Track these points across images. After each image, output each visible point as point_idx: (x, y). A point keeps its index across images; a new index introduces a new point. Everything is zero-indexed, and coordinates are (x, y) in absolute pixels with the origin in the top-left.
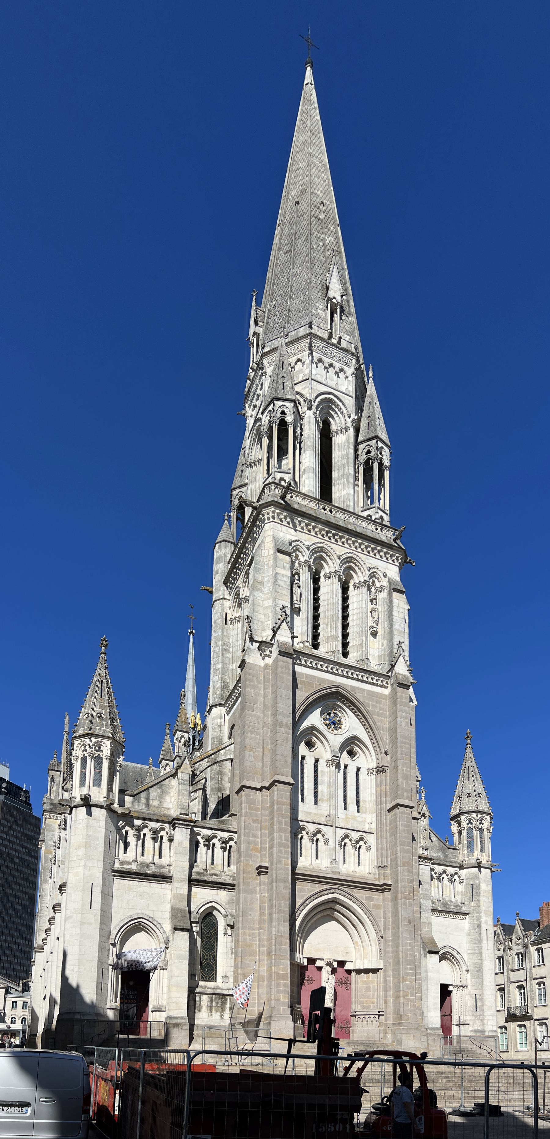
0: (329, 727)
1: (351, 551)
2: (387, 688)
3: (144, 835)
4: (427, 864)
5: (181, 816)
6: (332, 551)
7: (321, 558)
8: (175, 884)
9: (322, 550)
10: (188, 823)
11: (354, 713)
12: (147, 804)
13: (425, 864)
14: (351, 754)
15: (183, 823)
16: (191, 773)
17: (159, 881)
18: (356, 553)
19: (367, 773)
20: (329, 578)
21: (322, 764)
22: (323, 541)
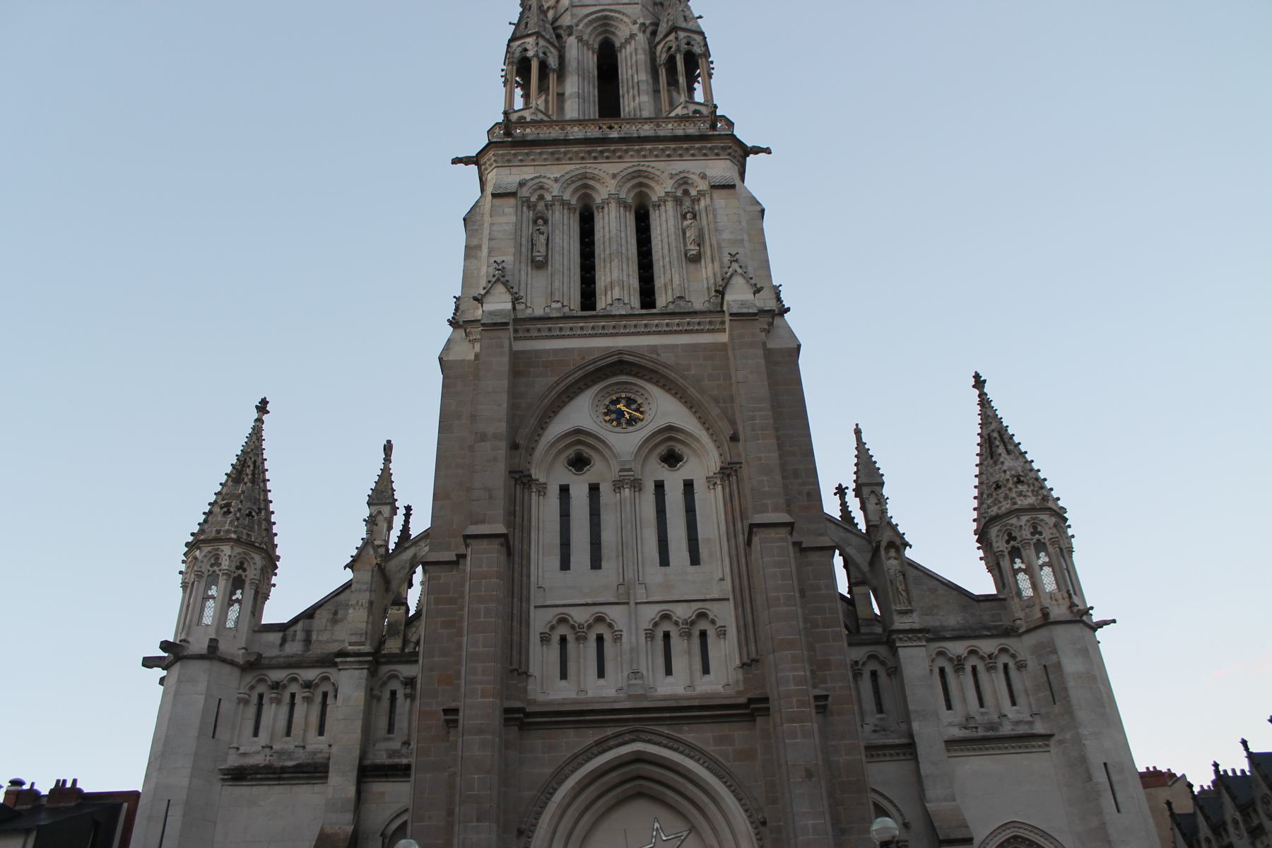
0: (615, 423)
1: (636, 164)
2: (724, 330)
3: (293, 696)
4: (915, 644)
5: (350, 648)
6: (601, 174)
7: (586, 186)
8: (334, 778)
9: (584, 176)
10: (361, 659)
11: (663, 387)
12: (308, 641)
13: (910, 644)
14: (672, 459)
15: (352, 659)
16: (376, 569)
17: (308, 778)
18: (647, 164)
19: (707, 485)
20: (603, 208)
21: (605, 489)
22: (584, 165)
